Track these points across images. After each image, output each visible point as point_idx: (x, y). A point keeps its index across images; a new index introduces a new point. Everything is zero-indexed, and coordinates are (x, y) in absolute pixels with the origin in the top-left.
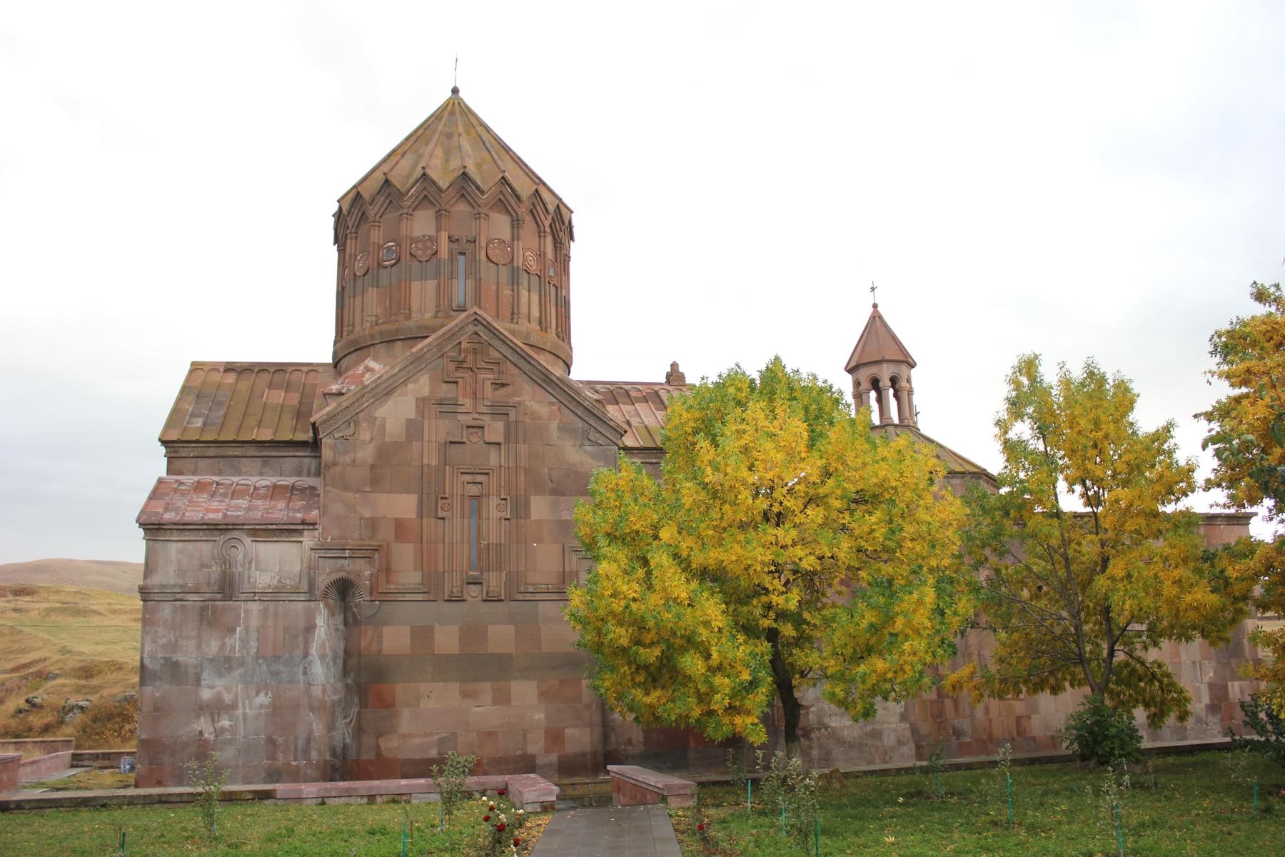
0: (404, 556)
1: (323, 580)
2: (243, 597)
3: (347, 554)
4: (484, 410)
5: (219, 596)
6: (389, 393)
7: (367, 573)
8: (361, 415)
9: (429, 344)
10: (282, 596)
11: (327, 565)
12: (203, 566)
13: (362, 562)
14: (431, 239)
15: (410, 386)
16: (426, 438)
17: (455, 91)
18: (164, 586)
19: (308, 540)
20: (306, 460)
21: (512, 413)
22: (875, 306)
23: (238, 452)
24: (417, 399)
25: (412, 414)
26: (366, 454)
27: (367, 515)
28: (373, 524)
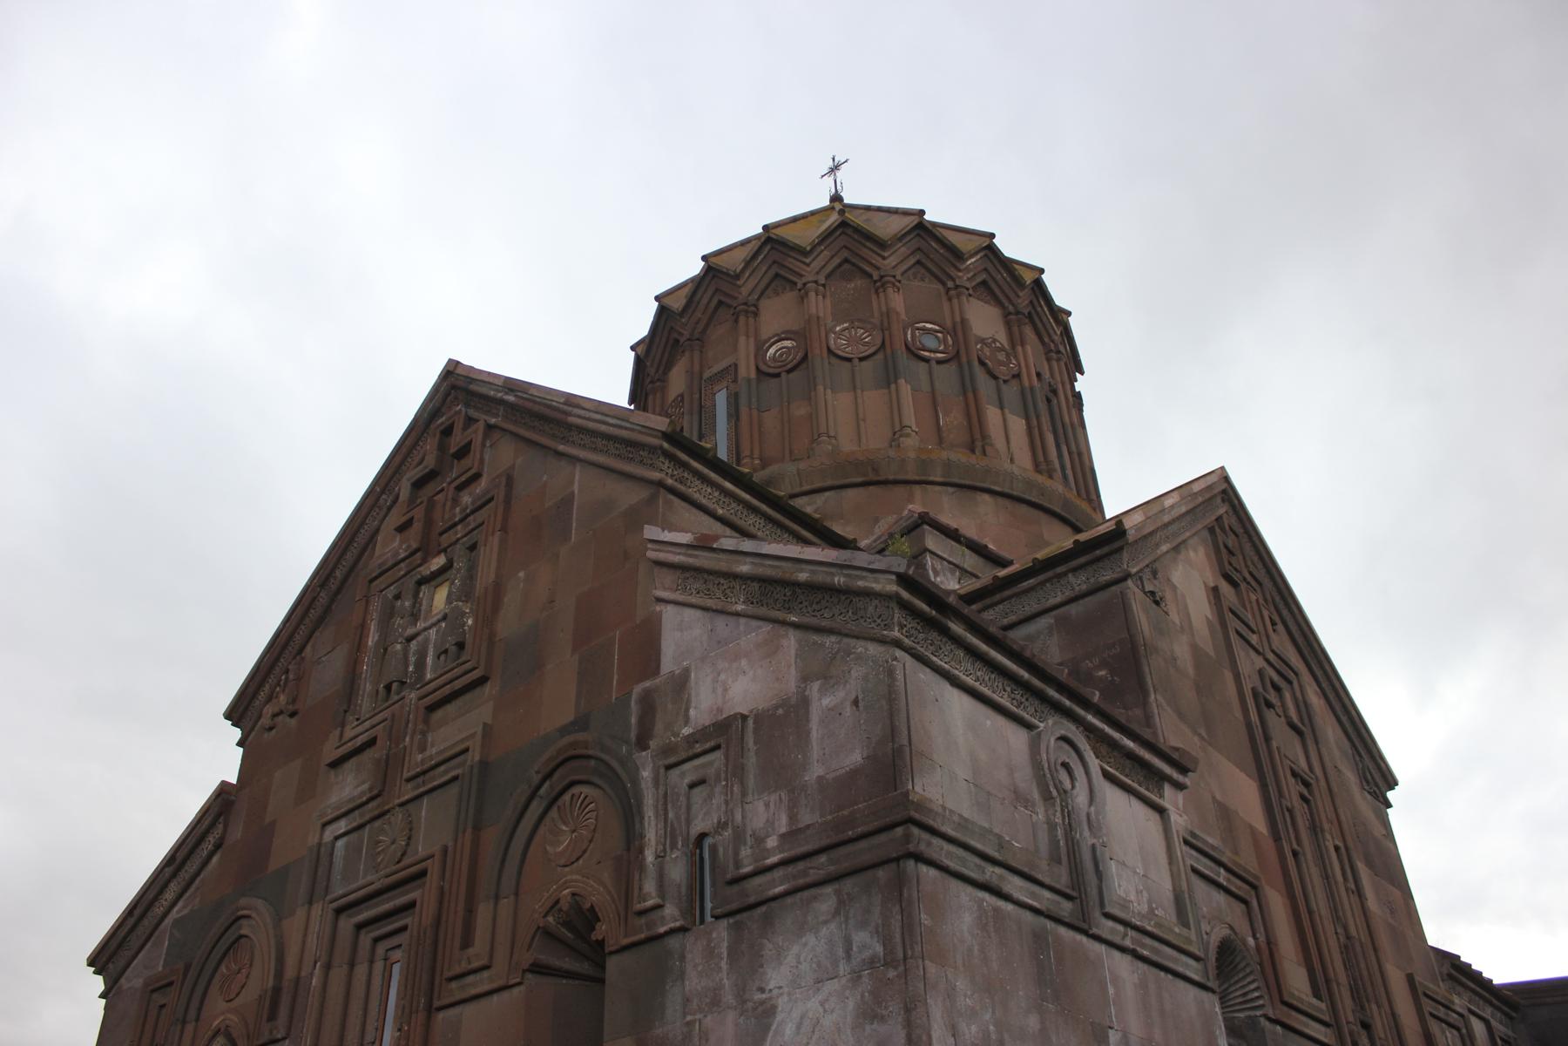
2: (1107, 928)
14: (1002, 349)
17: (836, 198)
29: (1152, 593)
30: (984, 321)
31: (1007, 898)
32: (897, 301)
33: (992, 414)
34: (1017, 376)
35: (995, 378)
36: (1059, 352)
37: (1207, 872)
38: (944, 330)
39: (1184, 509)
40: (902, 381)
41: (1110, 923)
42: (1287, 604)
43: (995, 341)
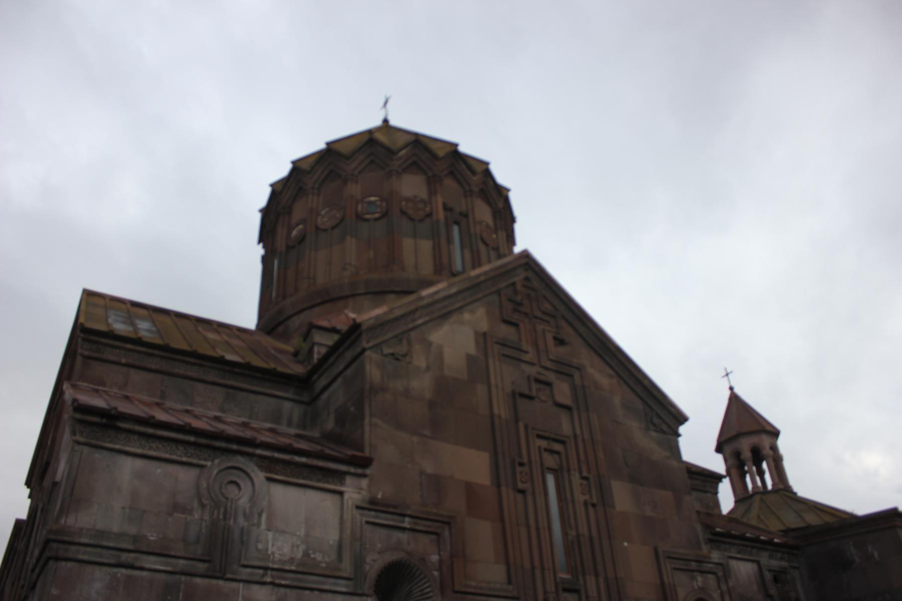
0: (481, 535)
1: (375, 563)
2: (245, 573)
3: (407, 523)
4: (549, 364)
5: (201, 567)
6: (445, 316)
7: (435, 558)
8: (413, 334)
9: (485, 273)
10: (312, 581)
11: (378, 538)
12: (176, 508)
13: (425, 539)
14: (422, 201)
15: (466, 316)
16: (493, 381)
17: (386, 121)
18: (102, 534)
19: (354, 491)
20: (287, 405)
21: (577, 376)
22: (731, 389)
23: (192, 372)
24: (476, 333)
25: (472, 349)
26: (422, 384)
27: (429, 470)
28: (437, 484)
29: (393, 354)
30: (411, 186)
31: (142, 569)
32: (354, 190)
33: (408, 243)
34: (430, 215)
35: (412, 220)
36: (471, 191)
37: (391, 523)
38: (382, 200)
39: (454, 290)
40: (348, 238)
41: (249, 570)
42: (584, 324)
43: (415, 197)
